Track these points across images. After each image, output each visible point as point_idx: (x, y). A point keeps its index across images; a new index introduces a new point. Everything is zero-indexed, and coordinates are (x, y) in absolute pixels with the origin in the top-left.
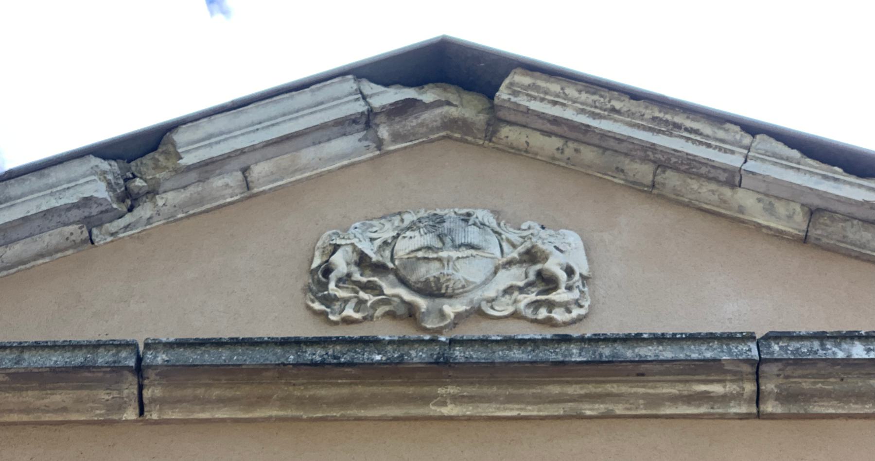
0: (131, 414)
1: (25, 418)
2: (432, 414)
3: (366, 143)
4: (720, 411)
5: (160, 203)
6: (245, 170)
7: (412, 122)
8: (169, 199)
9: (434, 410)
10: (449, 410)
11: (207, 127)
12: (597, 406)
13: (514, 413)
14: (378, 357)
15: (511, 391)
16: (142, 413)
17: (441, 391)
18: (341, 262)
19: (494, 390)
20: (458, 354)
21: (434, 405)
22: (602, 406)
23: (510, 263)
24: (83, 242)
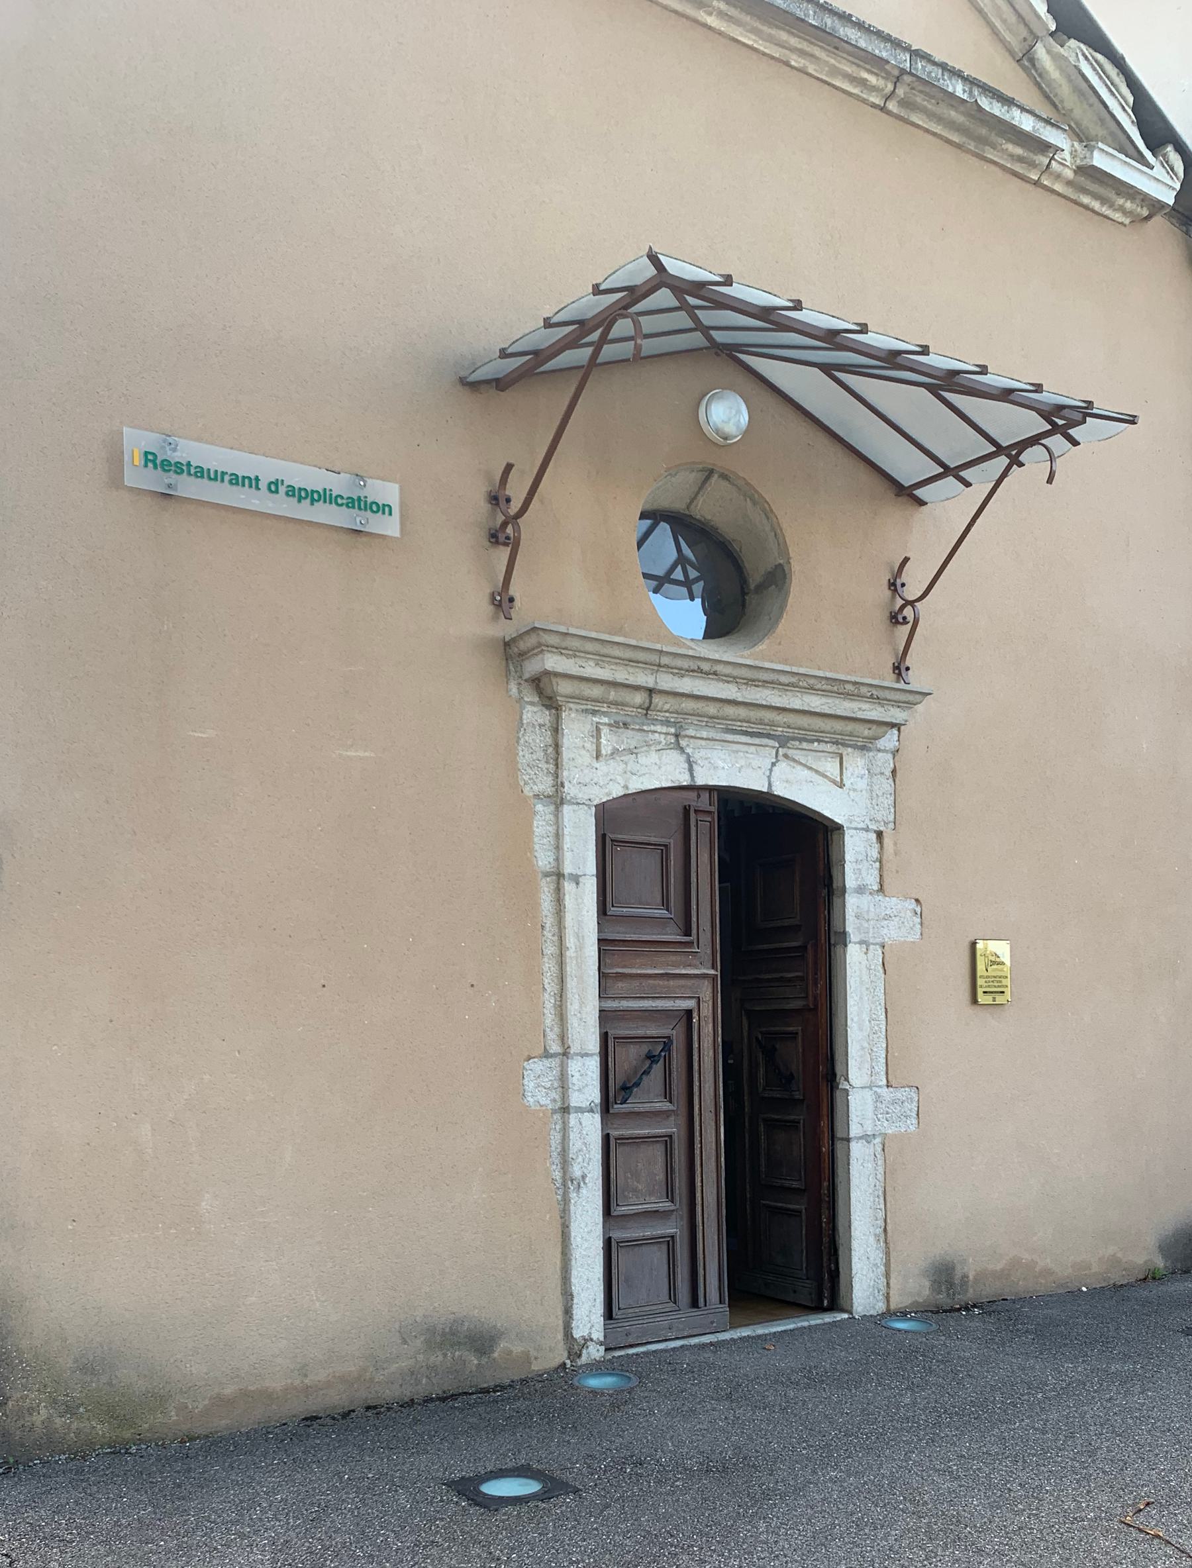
2: (700, 18)
4: (865, 96)
9: (702, 16)
10: (712, 21)
12: (800, 60)
13: (750, 43)
15: (757, 24)
19: (748, 18)
21: (705, 11)
22: (803, 61)
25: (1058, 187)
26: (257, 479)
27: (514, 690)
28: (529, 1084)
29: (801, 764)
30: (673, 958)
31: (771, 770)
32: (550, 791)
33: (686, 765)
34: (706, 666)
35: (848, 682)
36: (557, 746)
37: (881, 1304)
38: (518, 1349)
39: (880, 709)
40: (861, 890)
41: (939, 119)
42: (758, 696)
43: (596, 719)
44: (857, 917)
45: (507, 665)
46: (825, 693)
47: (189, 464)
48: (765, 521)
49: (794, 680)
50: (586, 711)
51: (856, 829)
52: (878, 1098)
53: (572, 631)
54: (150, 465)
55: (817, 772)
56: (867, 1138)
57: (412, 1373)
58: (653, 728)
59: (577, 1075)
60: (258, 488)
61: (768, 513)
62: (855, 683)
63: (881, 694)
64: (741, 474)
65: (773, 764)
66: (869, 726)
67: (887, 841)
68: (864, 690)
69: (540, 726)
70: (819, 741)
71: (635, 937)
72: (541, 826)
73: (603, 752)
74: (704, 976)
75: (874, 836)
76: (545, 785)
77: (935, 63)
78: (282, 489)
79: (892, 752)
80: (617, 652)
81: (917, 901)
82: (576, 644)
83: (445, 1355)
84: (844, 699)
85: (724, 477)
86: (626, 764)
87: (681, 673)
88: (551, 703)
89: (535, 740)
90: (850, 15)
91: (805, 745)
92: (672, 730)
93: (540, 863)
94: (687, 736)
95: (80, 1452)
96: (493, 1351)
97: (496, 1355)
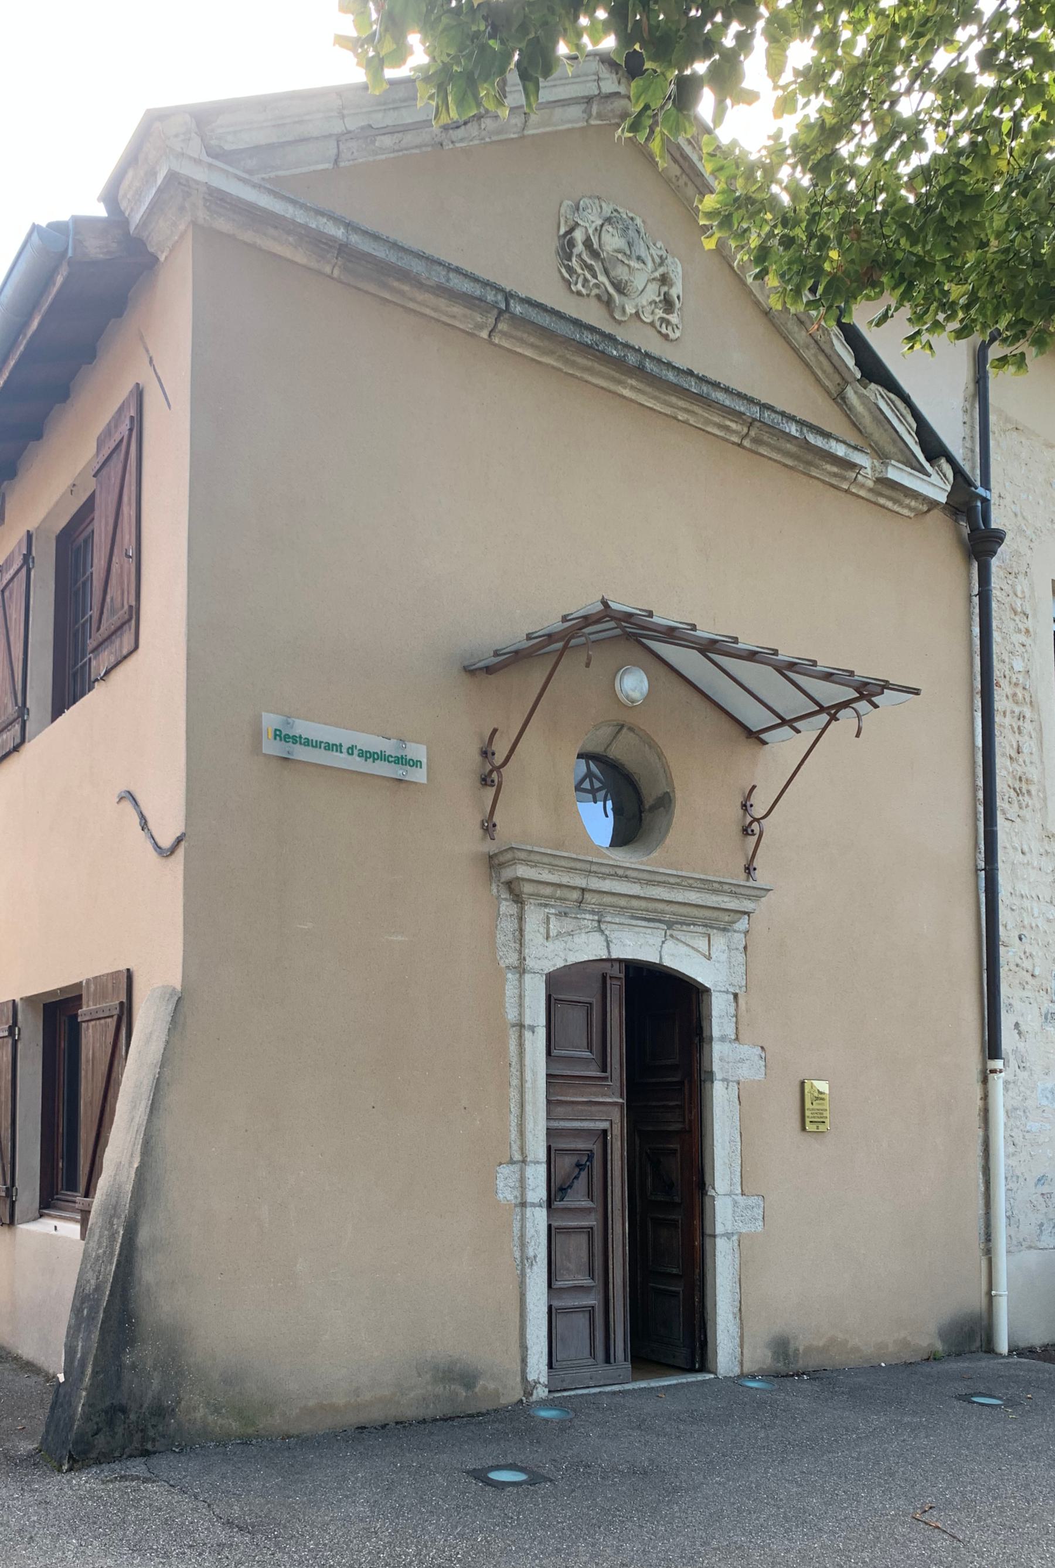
4: (727, 437)
15: (657, 394)
17: (629, 381)
20: (649, 365)
25: (862, 493)
26: (341, 745)
29: (682, 942)
30: (594, 1089)
31: (661, 947)
32: (516, 964)
33: (605, 944)
34: (620, 872)
35: (715, 882)
36: (521, 930)
38: (492, 1386)
40: (723, 1039)
41: (779, 450)
42: (654, 893)
43: (547, 910)
44: (721, 1060)
45: (491, 873)
46: (700, 890)
47: (300, 737)
48: (657, 761)
49: (678, 881)
50: (541, 905)
51: (720, 991)
53: (536, 849)
54: (278, 738)
55: (693, 948)
57: (424, 1399)
58: (583, 916)
60: (341, 752)
61: (660, 755)
62: (720, 883)
63: (738, 890)
64: (642, 727)
65: (663, 942)
66: (729, 913)
67: (741, 1001)
68: (726, 887)
69: (511, 915)
70: (694, 925)
71: (569, 1073)
72: (510, 990)
73: (551, 934)
75: (732, 997)
76: (512, 959)
77: (776, 412)
78: (356, 752)
80: (563, 863)
81: (762, 1048)
82: (537, 858)
83: (445, 1387)
84: (712, 894)
85: (631, 729)
86: (566, 943)
87: (604, 876)
88: (518, 899)
89: (508, 926)
90: (719, 383)
91: (685, 928)
92: (596, 918)
93: (509, 1017)
94: (605, 922)
96: (475, 1387)
97: (477, 1390)
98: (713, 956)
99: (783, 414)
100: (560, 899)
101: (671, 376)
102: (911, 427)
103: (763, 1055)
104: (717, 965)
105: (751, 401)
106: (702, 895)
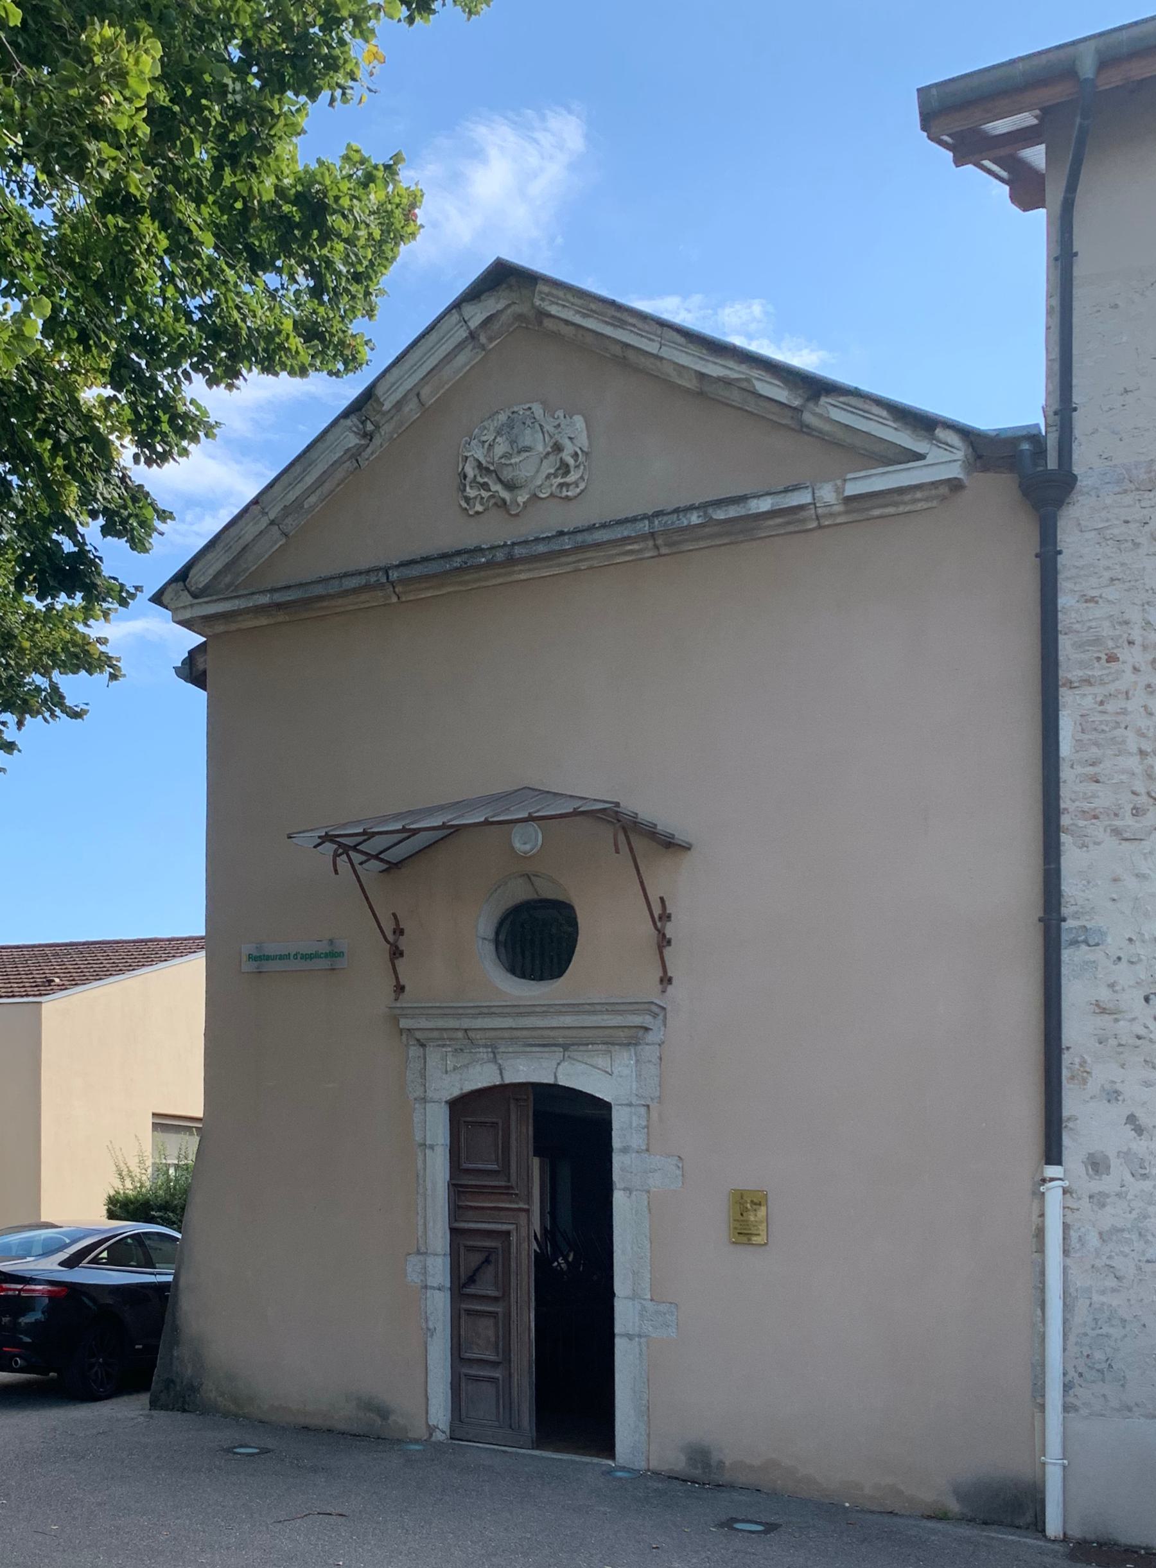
0: (394, 599)
1: (356, 607)
3: (475, 351)
5: (383, 433)
6: (418, 395)
7: (496, 326)
8: (386, 429)
10: (523, 576)
11: (390, 378)
14: (483, 560)
16: (399, 598)
18: (470, 471)
23: (548, 454)
24: (356, 468)
27: (404, 1037)
28: (409, 1270)
33: (498, 1072)
37: (643, 1463)
39: (621, 1017)
41: (702, 538)
49: (544, 1009)
50: (439, 1046)
52: (644, 1308)
56: (630, 1337)
58: (478, 1050)
59: (431, 1266)
65: (559, 1064)
68: (598, 1008)
70: (592, 1044)
74: (520, 1210)
75: (643, 1110)
79: (659, 1045)
87: (475, 1016)
91: (582, 1048)
95: (226, 1415)
97: (389, 1422)
98: (616, 1072)
99: (677, 511)
100: (450, 1039)
101: (541, 548)
102: (881, 417)
103: (680, 1165)
104: (619, 1079)
105: (634, 520)
106: (579, 1018)
